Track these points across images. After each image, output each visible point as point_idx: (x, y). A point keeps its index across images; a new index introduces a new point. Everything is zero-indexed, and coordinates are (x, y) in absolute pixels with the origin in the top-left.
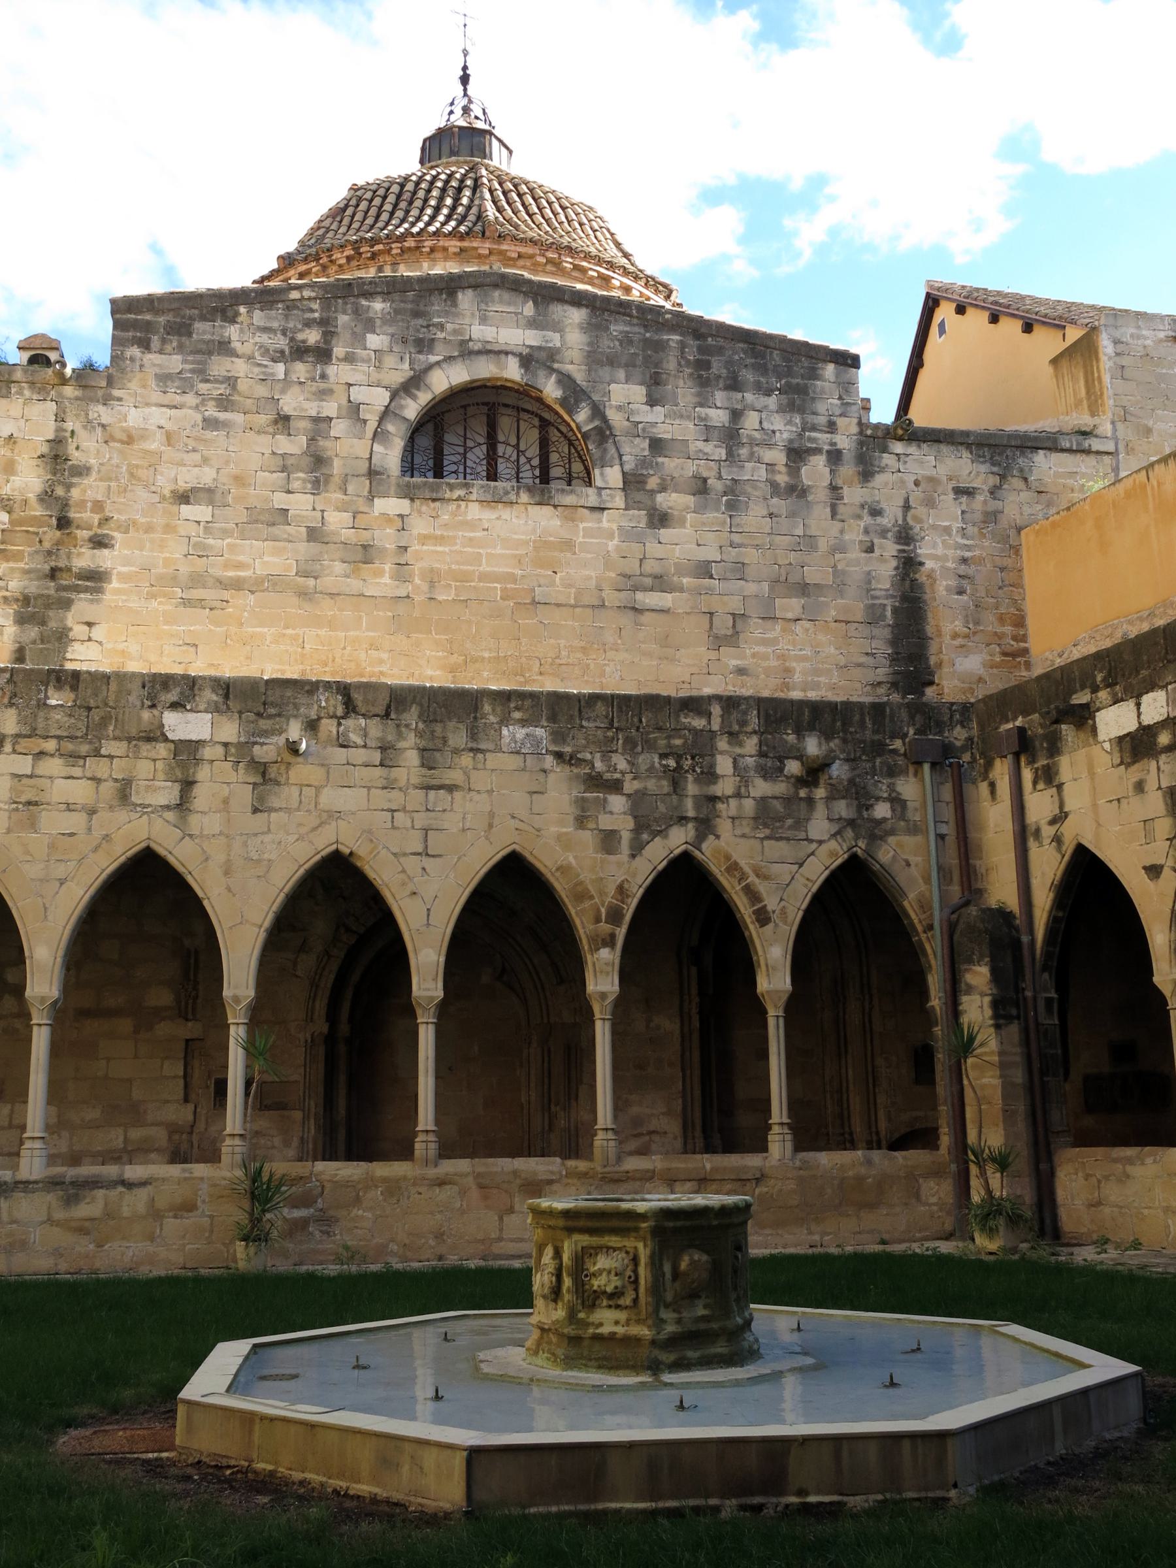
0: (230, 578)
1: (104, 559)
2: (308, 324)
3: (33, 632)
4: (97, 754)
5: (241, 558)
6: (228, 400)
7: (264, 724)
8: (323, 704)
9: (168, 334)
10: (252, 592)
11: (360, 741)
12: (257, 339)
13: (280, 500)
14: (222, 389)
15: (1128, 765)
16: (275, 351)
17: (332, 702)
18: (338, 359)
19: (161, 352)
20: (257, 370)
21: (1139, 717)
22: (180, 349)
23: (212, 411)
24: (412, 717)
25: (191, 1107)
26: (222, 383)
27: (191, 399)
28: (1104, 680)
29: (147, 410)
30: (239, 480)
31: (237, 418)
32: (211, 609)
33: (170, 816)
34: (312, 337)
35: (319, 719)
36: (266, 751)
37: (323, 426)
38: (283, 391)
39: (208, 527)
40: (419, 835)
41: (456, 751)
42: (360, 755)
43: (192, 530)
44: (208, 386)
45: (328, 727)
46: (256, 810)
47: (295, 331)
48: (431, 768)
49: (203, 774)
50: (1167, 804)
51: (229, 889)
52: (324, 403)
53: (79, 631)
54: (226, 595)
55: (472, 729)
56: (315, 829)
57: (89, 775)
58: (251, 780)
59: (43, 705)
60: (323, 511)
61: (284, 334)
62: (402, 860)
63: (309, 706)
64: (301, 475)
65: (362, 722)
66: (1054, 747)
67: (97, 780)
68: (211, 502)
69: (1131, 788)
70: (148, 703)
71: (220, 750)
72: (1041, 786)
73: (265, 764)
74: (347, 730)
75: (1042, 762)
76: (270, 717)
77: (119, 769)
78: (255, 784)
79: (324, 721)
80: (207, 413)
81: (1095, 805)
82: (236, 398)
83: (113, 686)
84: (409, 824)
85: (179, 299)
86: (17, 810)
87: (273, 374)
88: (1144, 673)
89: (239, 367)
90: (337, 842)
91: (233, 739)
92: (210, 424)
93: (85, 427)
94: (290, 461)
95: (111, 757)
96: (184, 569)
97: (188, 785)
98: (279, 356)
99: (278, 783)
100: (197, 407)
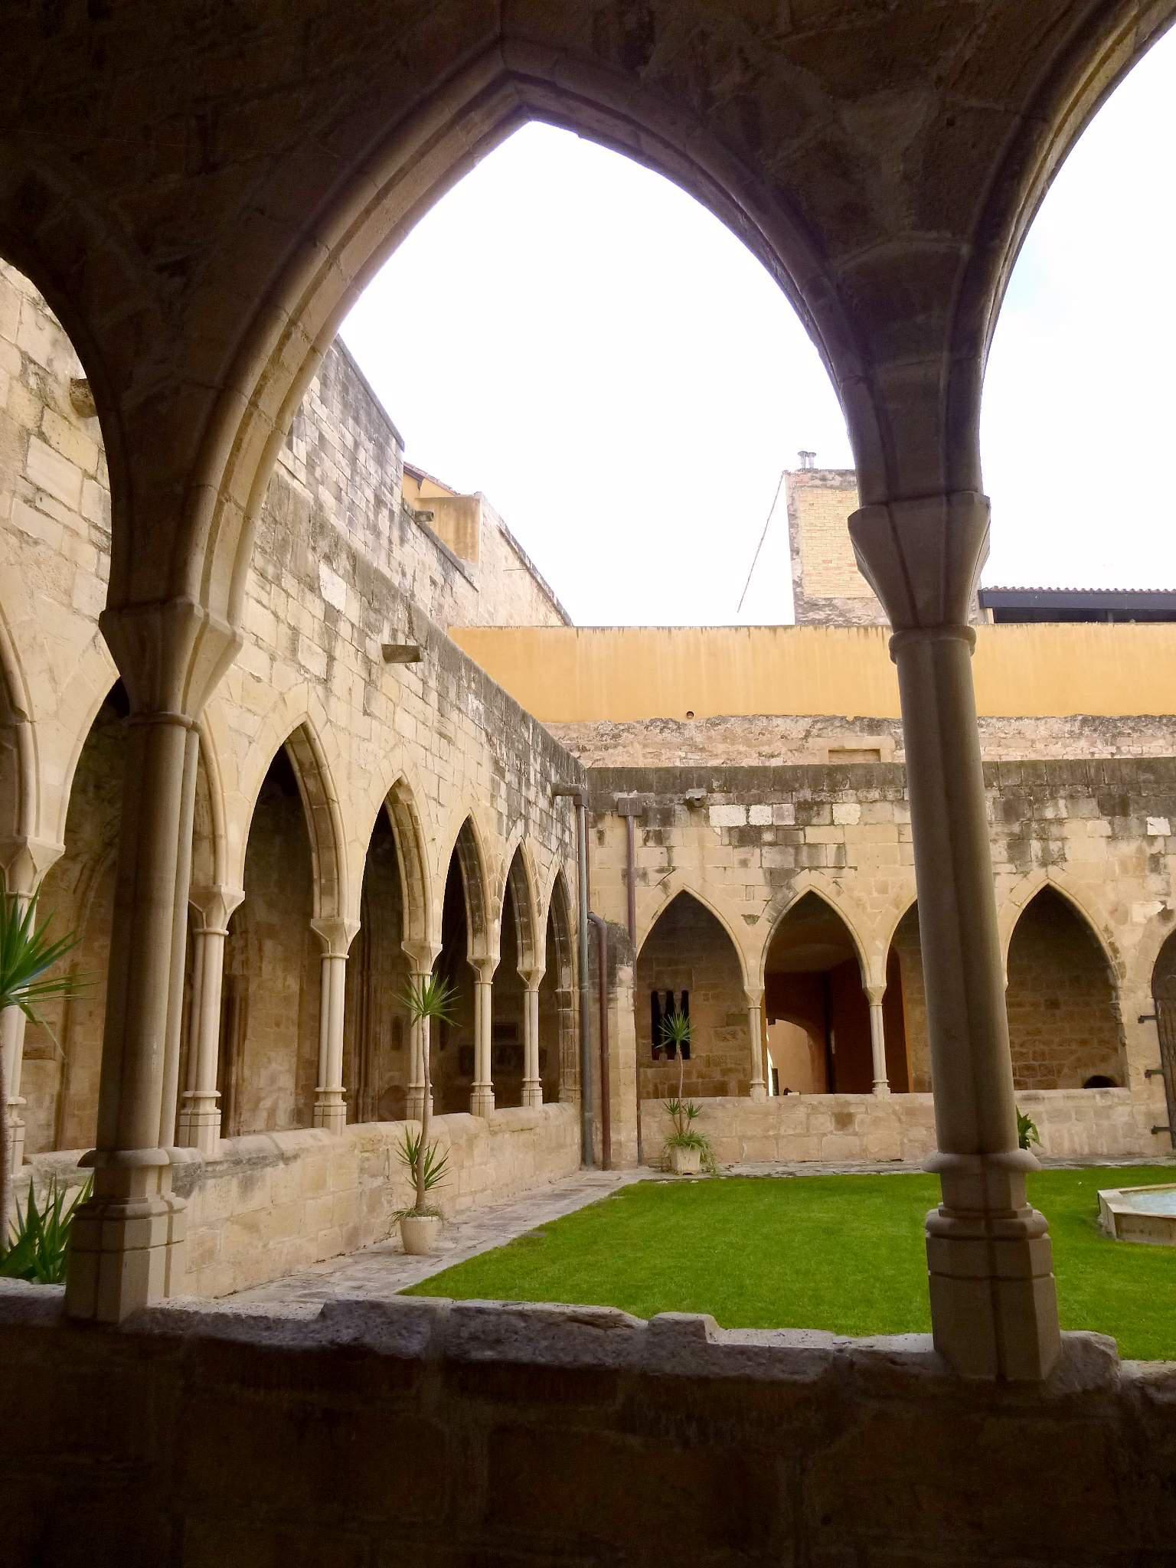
15: (736, 847)
21: (748, 817)
28: (720, 786)
50: (766, 878)
66: (667, 817)
69: (736, 862)
72: (651, 843)
75: (654, 827)
81: (703, 868)
88: (754, 791)
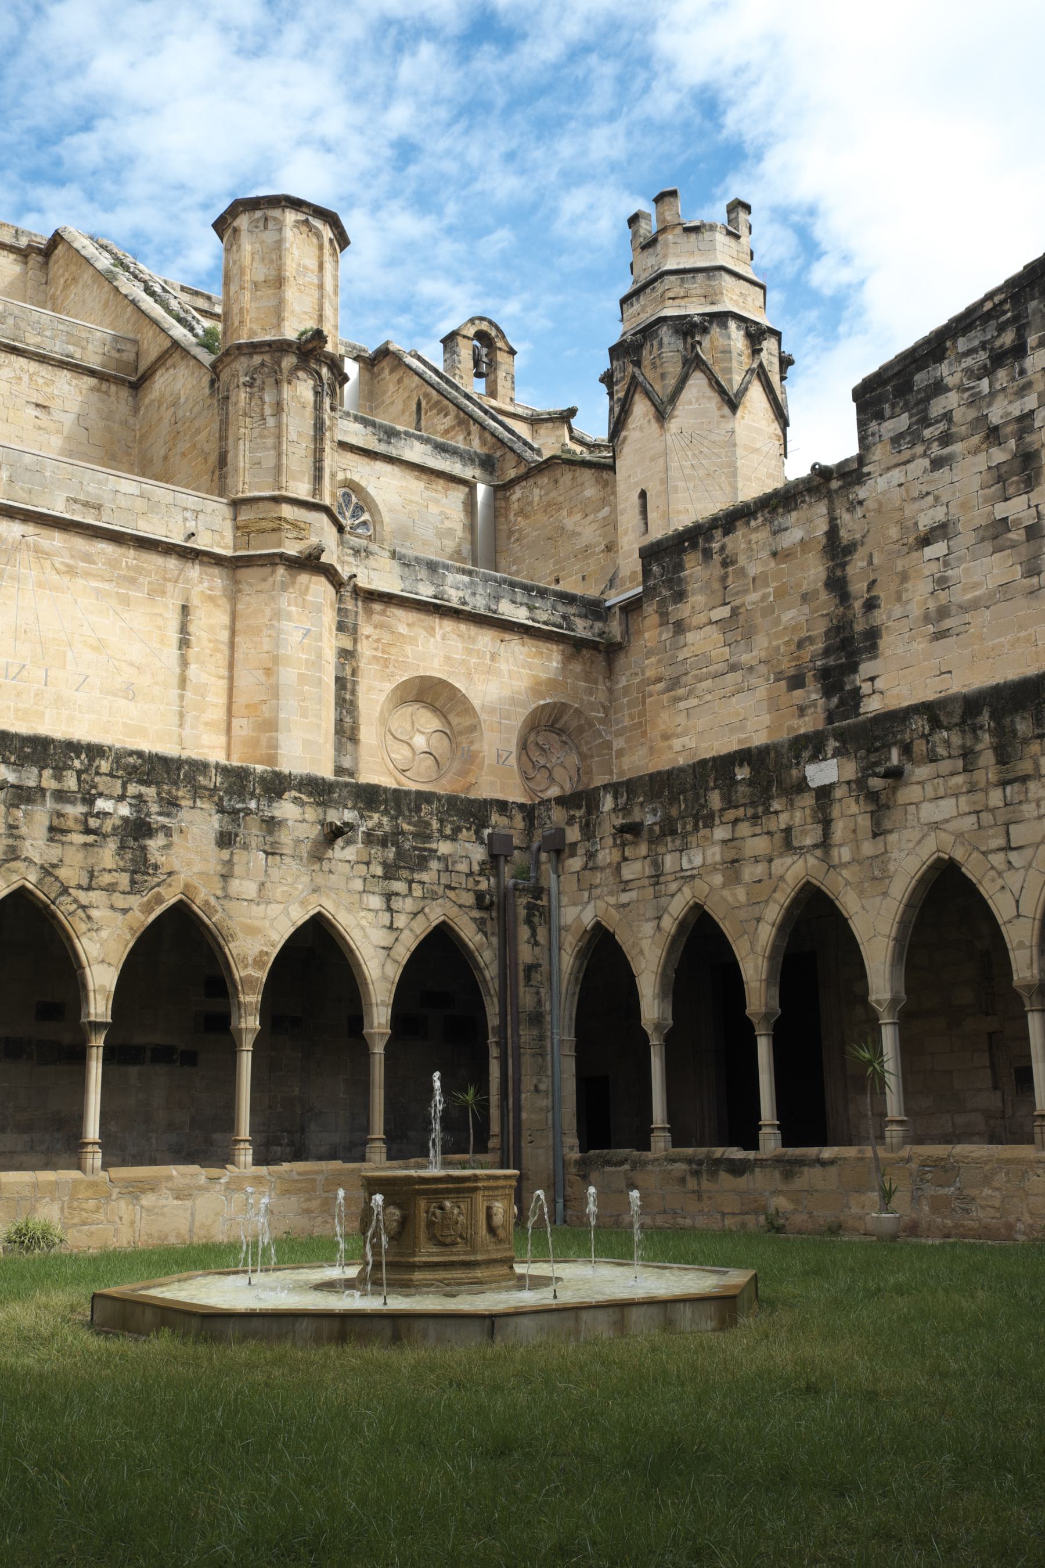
0: (969, 600)
1: (879, 617)
2: (1001, 329)
3: (835, 700)
4: (767, 812)
5: (975, 579)
6: (947, 435)
7: (873, 758)
8: (914, 727)
9: (895, 397)
10: (988, 607)
11: (945, 753)
12: (964, 365)
13: (1001, 510)
14: (942, 426)
16: (978, 369)
17: (920, 723)
18: (1032, 349)
19: (891, 417)
20: (966, 395)
22: (906, 408)
23: (936, 450)
24: (985, 718)
25: (999, 1093)
26: (941, 421)
27: (919, 449)
29: (889, 475)
30: (964, 506)
31: (957, 448)
32: (958, 635)
33: (818, 852)
34: (1008, 338)
35: (912, 742)
36: (876, 783)
37: (1027, 422)
38: (989, 405)
39: (945, 561)
40: (1001, 830)
41: (1026, 741)
42: (945, 766)
43: (934, 568)
44: (931, 429)
45: (920, 747)
46: (875, 835)
47: (994, 338)
48: (1005, 764)
49: (836, 811)
51: (863, 908)
52: (1026, 399)
53: (866, 688)
54: (967, 618)
55: (1036, 715)
56: (919, 842)
57: (765, 830)
58: (869, 809)
59: (734, 782)
60: (1037, 506)
61: (984, 348)
62: (990, 857)
63: (903, 732)
64: (1015, 478)
65: (945, 734)
67: (768, 833)
68: (946, 537)
70: (794, 761)
71: (845, 787)
73: (877, 792)
74: (934, 746)
76: (877, 750)
77: (784, 819)
78: (872, 812)
79: (917, 742)
80: (933, 455)
82: (954, 430)
83: (772, 755)
84: (992, 822)
85: (899, 361)
86: (727, 868)
87: (980, 392)
89: (951, 400)
90: (938, 851)
91: (853, 777)
92: (937, 464)
93: (848, 510)
94: (1004, 468)
95: (776, 812)
96: (932, 605)
97: (827, 823)
98: (987, 371)
99: (888, 808)
100: (925, 452)
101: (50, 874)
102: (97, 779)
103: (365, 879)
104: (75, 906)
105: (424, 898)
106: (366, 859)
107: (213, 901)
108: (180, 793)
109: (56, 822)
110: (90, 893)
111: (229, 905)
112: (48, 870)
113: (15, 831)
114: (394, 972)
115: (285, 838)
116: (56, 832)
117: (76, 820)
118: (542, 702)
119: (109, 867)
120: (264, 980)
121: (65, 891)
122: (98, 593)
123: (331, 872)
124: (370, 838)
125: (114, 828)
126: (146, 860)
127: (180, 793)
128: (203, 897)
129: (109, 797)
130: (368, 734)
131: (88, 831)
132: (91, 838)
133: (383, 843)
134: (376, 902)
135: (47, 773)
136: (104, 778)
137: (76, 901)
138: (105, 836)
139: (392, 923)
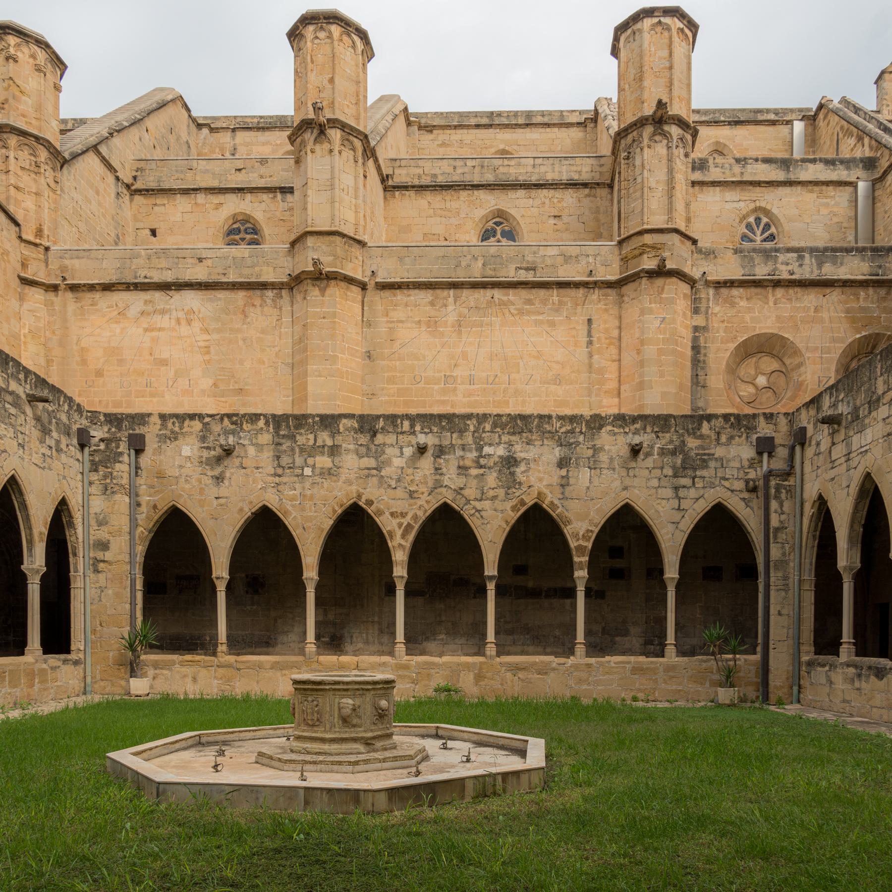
101: (460, 494)
102: (484, 435)
103: (660, 479)
104: (474, 511)
105: (704, 487)
106: (660, 465)
107: (556, 502)
108: (534, 437)
109: (461, 463)
110: (482, 502)
111: (566, 503)
112: (459, 491)
113: (440, 471)
114: (681, 539)
115: (603, 457)
116: (463, 469)
117: (473, 461)
118: (858, 336)
119: (492, 486)
120: (590, 547)
121: (468, 502)
122: (537, 323)
123: (635, 476)
124: (663, 452)
125: (495, 464)
126: (515, 480)
127: (534, 437)
128: (551, 499)
129: (490, 445)
130: (716, 380)
131: (481, 467)
132: (481, 471)
133: (673, 453)
134: (669, 493)
135: (455, 436)
136: (488, 434)
137: (474, 508)
138: (489, 468)
139: (679, 506)
